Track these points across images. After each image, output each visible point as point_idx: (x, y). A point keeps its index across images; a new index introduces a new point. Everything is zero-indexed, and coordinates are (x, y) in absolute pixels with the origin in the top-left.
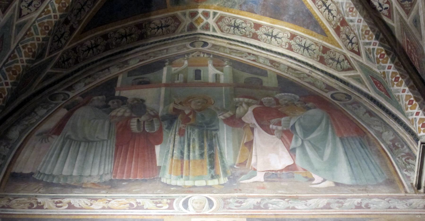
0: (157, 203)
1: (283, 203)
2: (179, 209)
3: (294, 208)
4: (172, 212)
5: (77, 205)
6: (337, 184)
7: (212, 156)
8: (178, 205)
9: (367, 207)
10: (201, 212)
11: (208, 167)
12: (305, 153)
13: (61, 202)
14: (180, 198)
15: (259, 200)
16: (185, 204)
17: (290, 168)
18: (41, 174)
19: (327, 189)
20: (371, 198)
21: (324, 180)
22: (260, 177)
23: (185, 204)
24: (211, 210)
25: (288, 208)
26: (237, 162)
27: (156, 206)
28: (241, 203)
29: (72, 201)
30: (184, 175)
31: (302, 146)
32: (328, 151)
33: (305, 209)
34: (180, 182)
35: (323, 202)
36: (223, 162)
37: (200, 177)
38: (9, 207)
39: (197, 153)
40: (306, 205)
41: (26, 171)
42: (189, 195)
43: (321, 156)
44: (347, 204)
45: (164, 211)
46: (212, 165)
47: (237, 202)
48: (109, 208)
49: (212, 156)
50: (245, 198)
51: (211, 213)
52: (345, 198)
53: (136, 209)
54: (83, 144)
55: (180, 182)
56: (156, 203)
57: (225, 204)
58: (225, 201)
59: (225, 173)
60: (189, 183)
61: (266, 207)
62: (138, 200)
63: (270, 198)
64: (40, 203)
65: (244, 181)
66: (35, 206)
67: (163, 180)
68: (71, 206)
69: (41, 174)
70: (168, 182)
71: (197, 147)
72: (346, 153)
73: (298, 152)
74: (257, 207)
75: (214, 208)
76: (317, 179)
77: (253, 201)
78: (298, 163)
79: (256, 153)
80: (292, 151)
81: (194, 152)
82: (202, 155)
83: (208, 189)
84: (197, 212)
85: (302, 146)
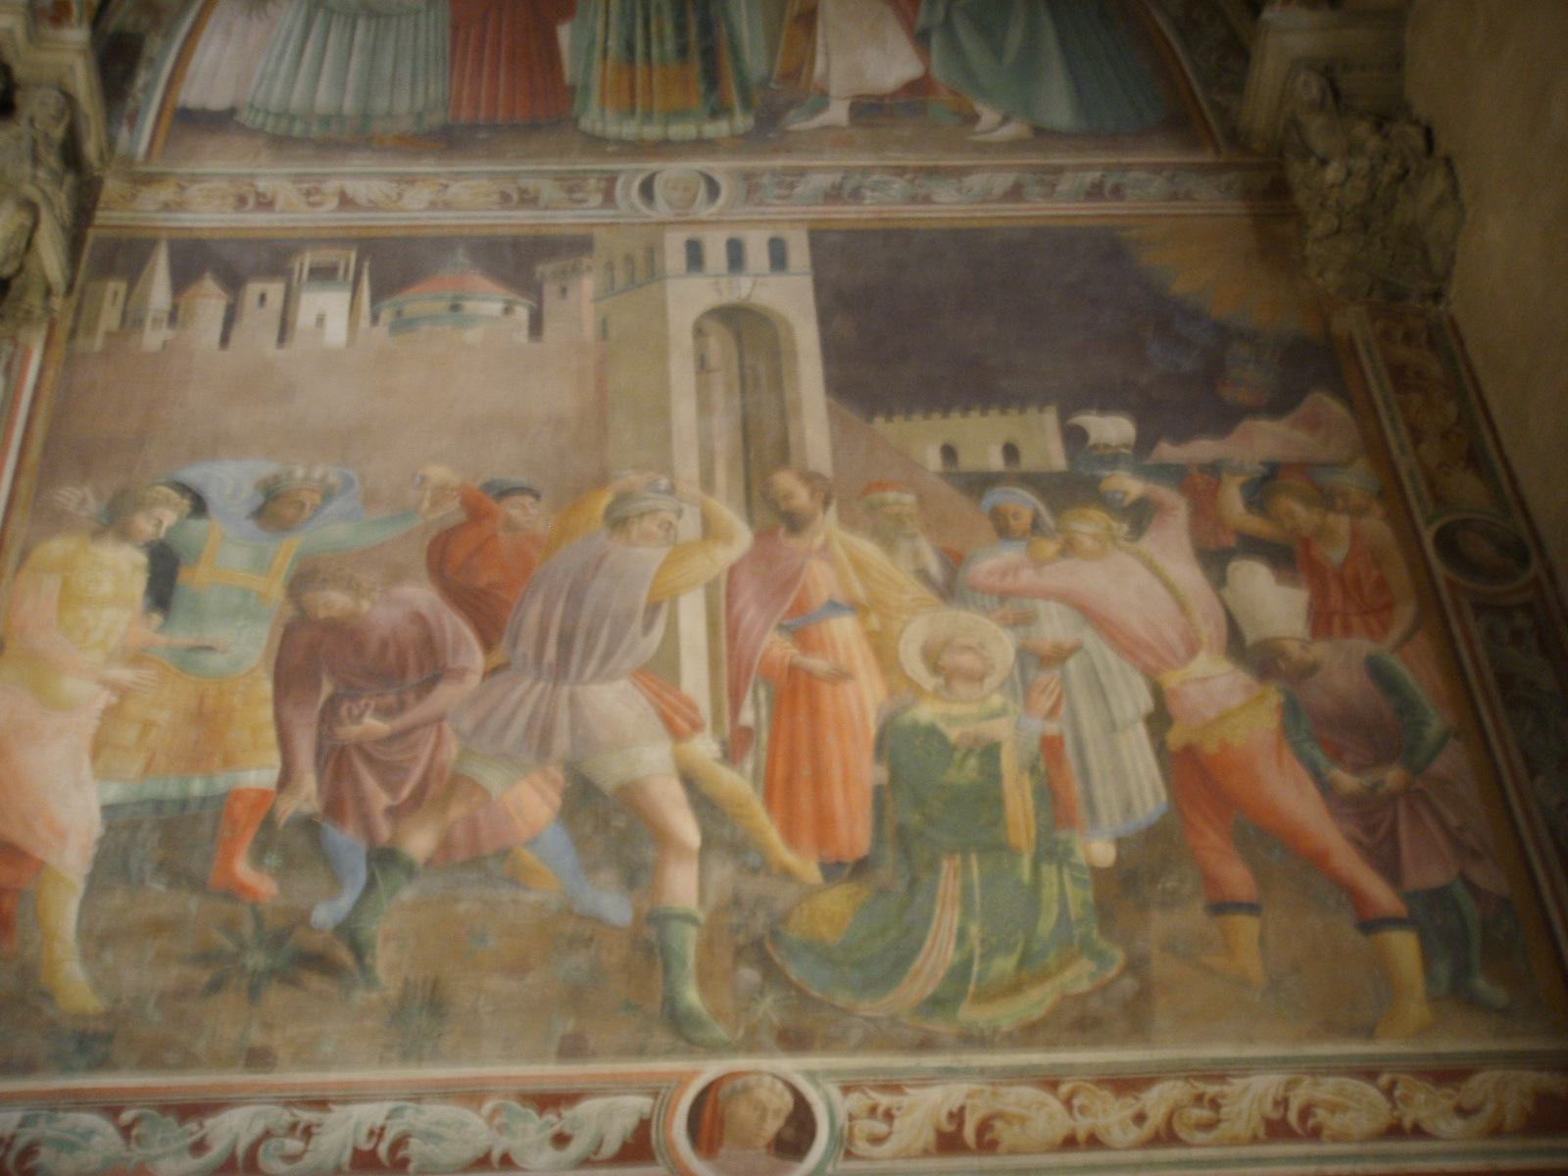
0: (572, 185)
1: (898, 185)
2: (632, 207)
3: (927, 200)
4: (613, 217)
5: (362, 199)
6: (1039, 132)
7: (710, 55)
8: (628, 192)
9: (1117, 192)
10: (687, 214)
11: (702, 88)
12: (954, 46)
13: (317, 191)
14: (631, 172)
15: (836, 178)
16: (647, 190)
17: (917, 90)
18: (258, 111)
19: (1014, 146)
20: (1126, 168)
21: (1006, 120)
22: (838, 112)
23: (647, 190)
24: (714, 209)
25: (913, 199)
26: (778, 69)
27: (570, 199)
28: (792, 186)
29: (353, 187)
30: (639, 109)
31: (947, 24)
32: (1015, 37)
33: (957, 203)
34: (630, 129)
35: (1003, 181)
36: (740, 72)
37: (680, 114)
38: (181, 206)
39: (670, 45)
40: (959, 190)
41: (218, 101)
42: (652, 165)
43: (998, 51)
44: (1065, 184)
45: (592, 213)
46: (712, 78)
47: (780, 184)
48: (448, 206)
49: (710, 55)
50: (802, 172)
51: (713, 218)
52: (1059, 170)
53: (517, 207)
54: (361, 23)
55: (630, 129)
56: (571, 190)
57: (749, 192)
58: (750, 182)
59: (747, 103)
60: (653, 131)
61: (856, 195)
62: (525, 183)
63: (866, 171)
64: (263, 195)
65: (798, 123)
66: (251, 201)
67: (585, 123)
68: (345, 201)
69: (258, 111)
70: (598, 127)
71: (669, 30)
72: (1063, 42)
73: (936, 42)
74: (833, 195)
75: (721, 201)
76: (988, 116)
77: (820, 181)
78: (938, 74)
79: (826, 46)
80: (921, 40)
81: (662, 42)
82: (683, 51)
83: (701, 146)
84: (679, 215)
85: (947, 24)
